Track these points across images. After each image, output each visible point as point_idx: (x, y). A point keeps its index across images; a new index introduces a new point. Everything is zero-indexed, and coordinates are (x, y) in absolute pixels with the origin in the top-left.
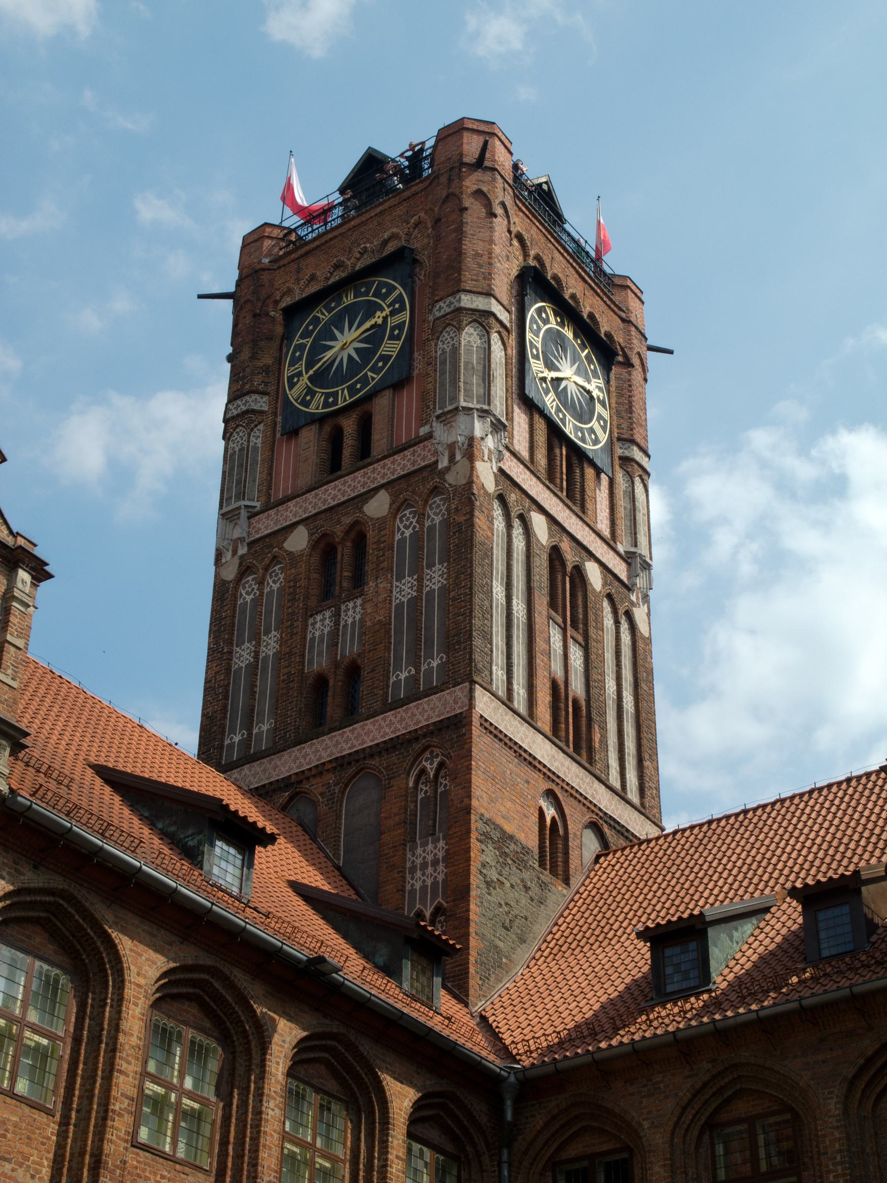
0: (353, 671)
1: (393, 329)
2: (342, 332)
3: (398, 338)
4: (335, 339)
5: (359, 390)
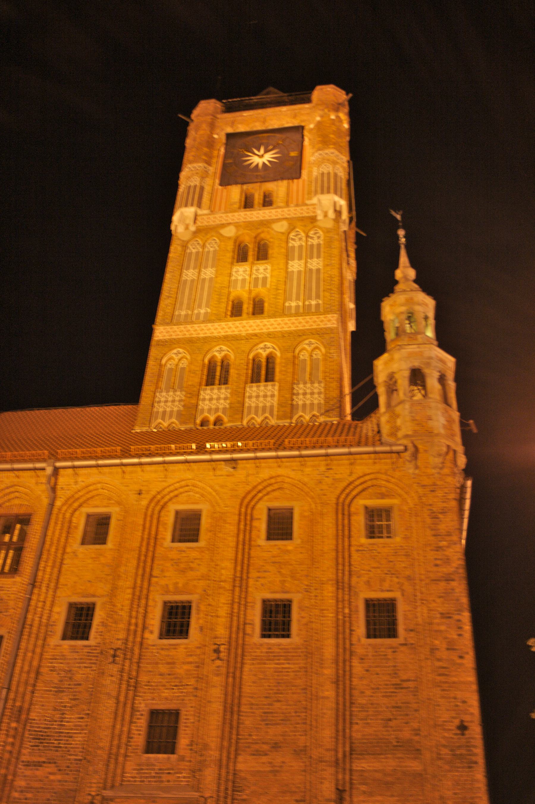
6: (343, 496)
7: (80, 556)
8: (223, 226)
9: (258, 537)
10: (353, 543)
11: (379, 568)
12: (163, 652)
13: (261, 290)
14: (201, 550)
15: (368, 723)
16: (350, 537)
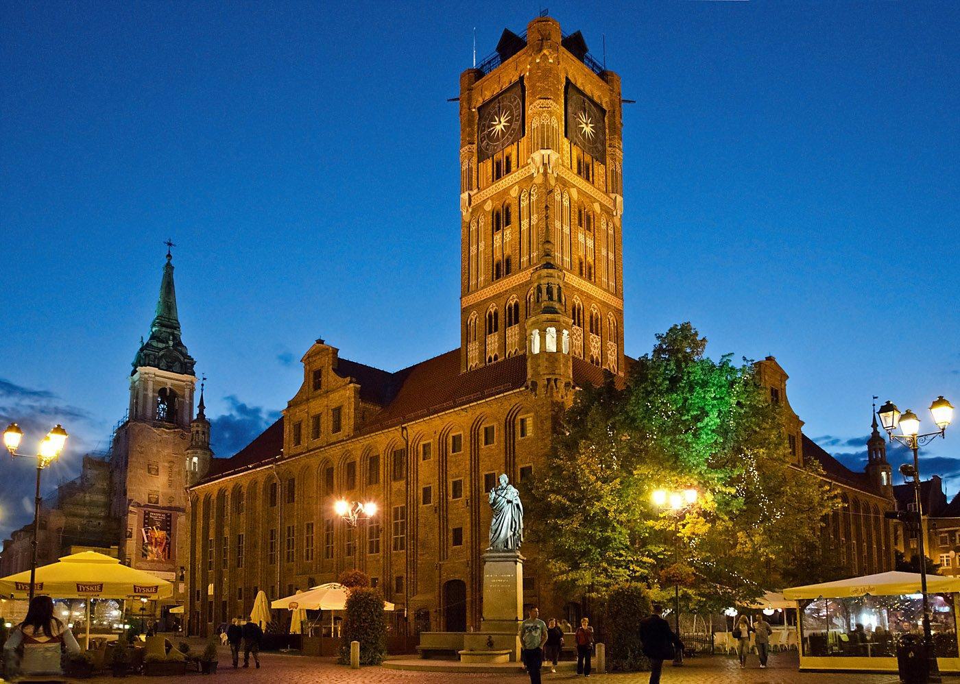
6: (509, 417)
8: (485, 202)
10: (516, 440)
13: (508, 251)
16: (514, 438)
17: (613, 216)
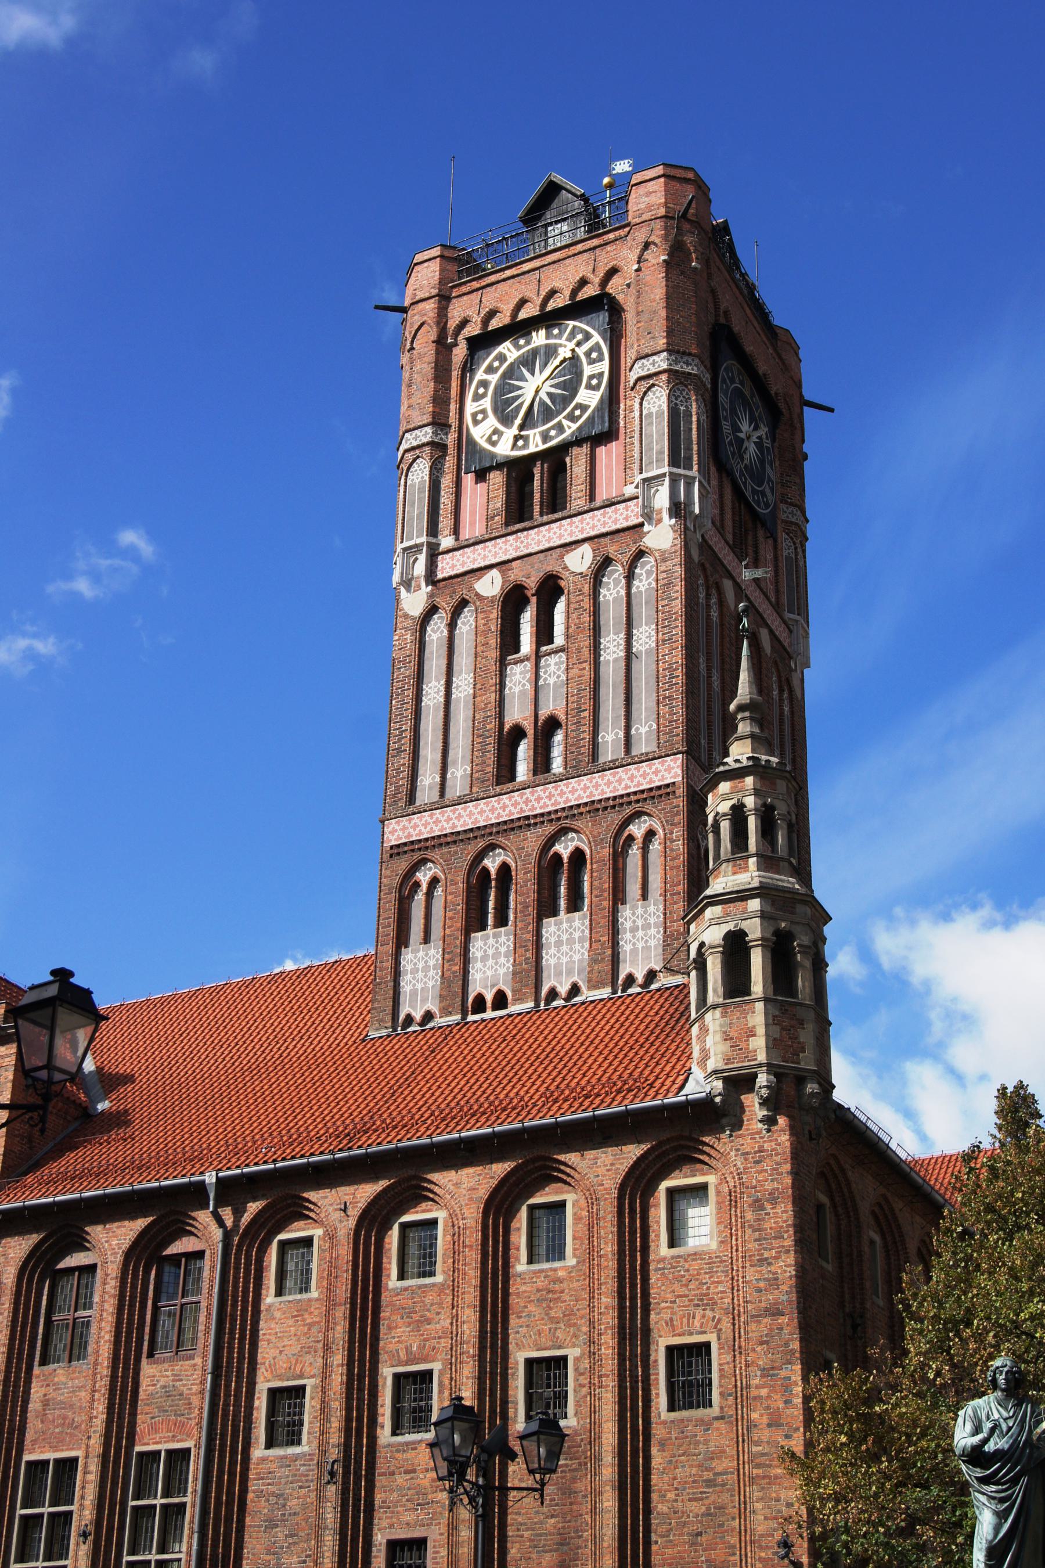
0: (552, 724)
1: (591, 377)
2: (533, 374)
3: (596, 388)
4: (523, 379)
5: (552, 438)
7: (278, 1315)
9: (518, 1259)
10: (652, 1257)
11: (687, 1296)
12: (399, 1456)
14: (441, 1288)
15: (671, 1541)
17: (791, 670)
